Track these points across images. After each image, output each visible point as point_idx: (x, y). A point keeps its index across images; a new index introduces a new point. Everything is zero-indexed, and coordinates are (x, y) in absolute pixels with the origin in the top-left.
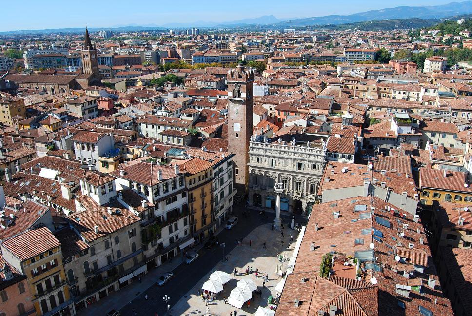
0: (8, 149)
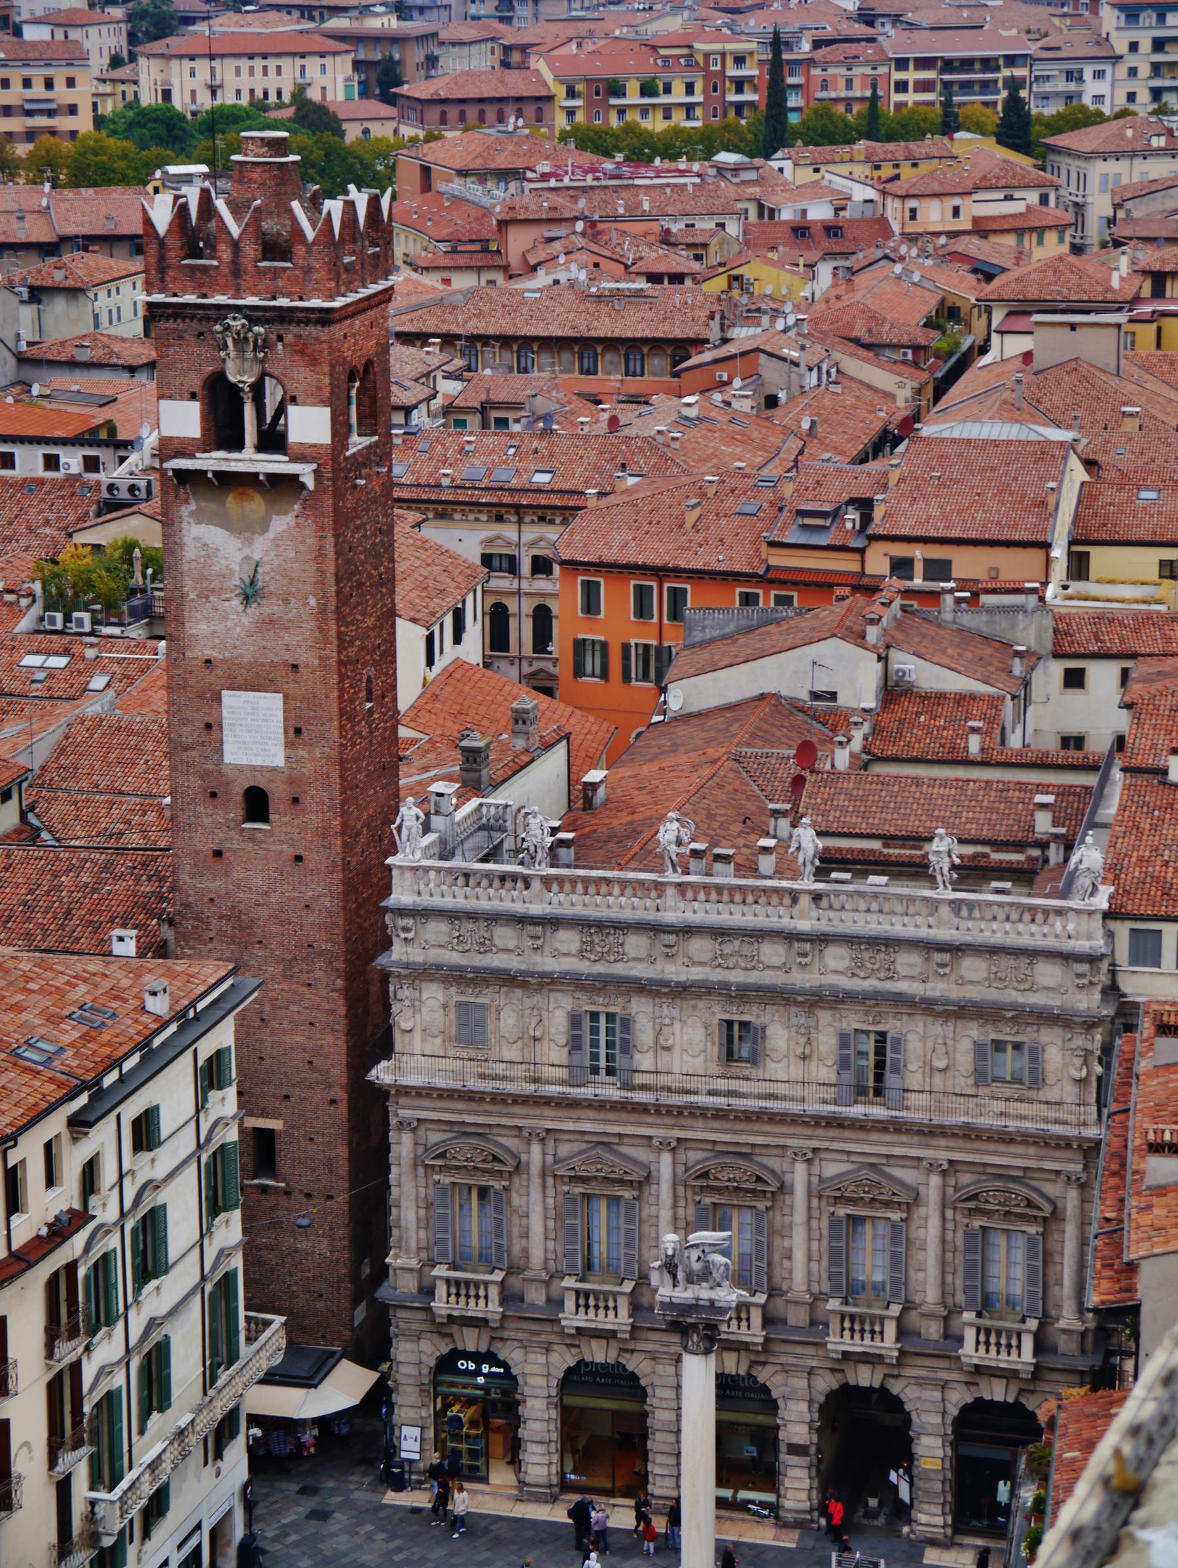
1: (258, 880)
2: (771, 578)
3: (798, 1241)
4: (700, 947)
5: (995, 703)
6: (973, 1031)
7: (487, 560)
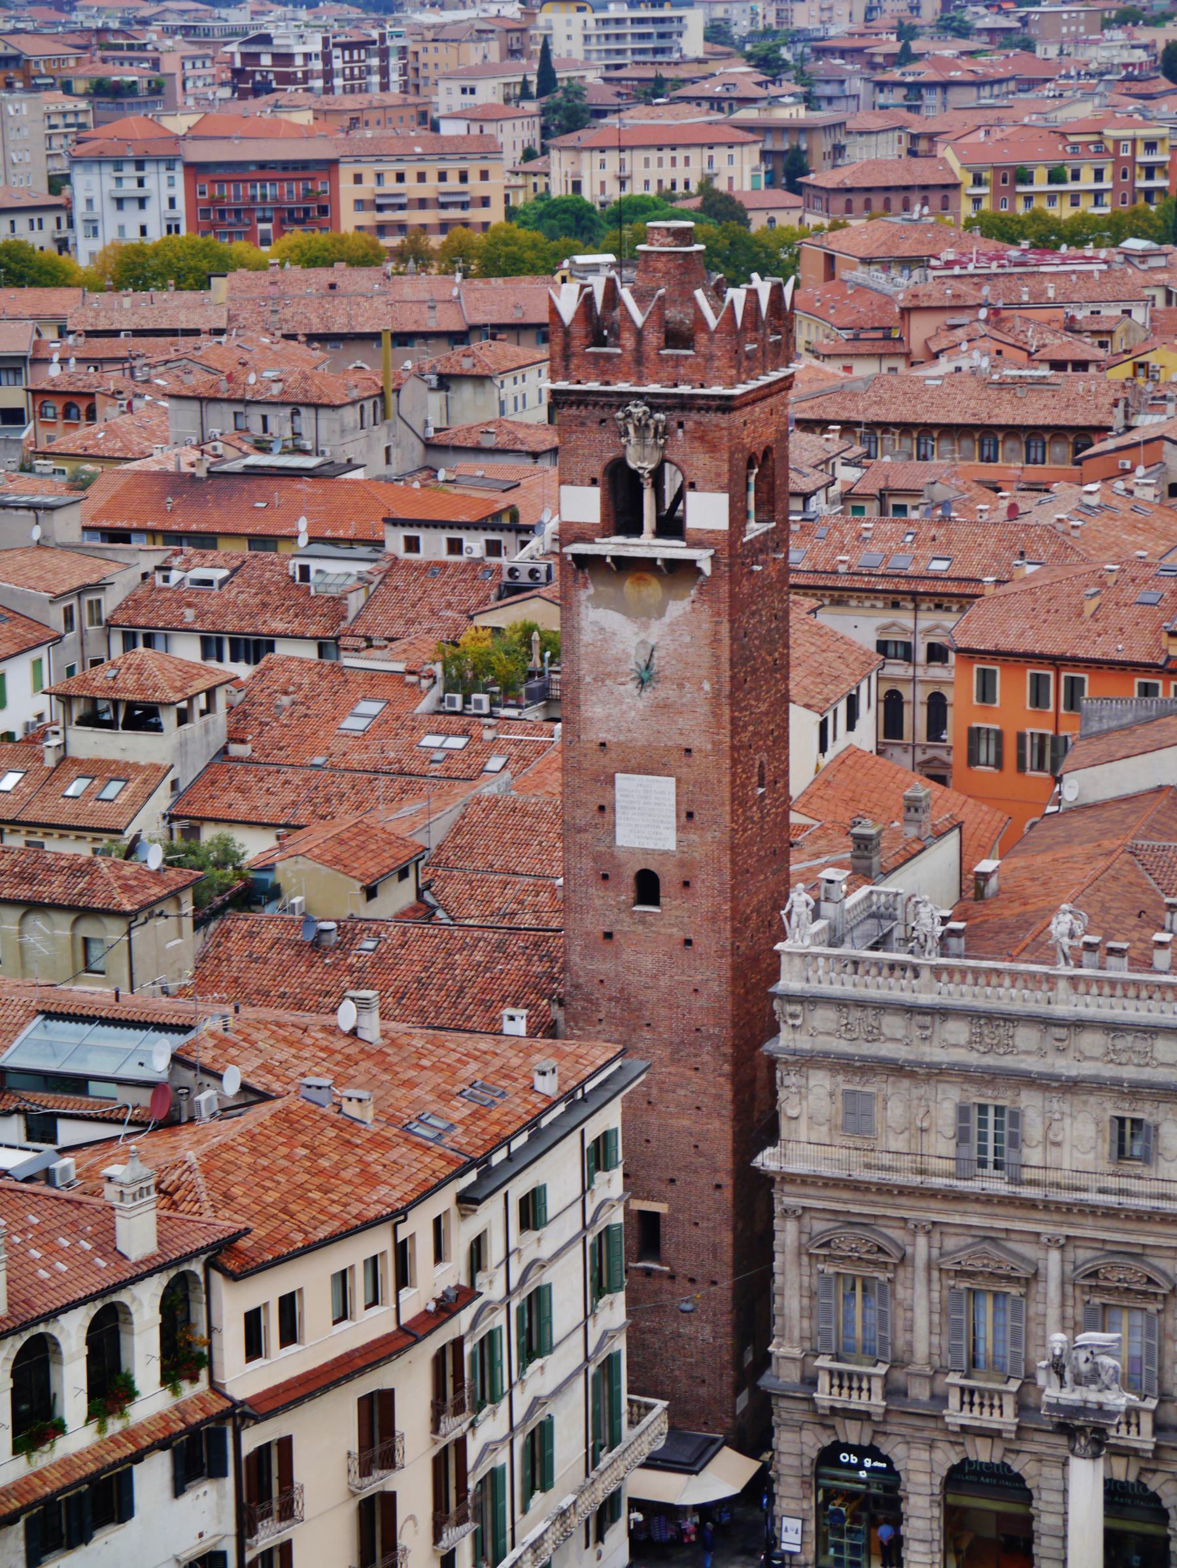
0: (500, 574)
1: (648, 963)
4: (1092, 1042)
7: (882, 647)
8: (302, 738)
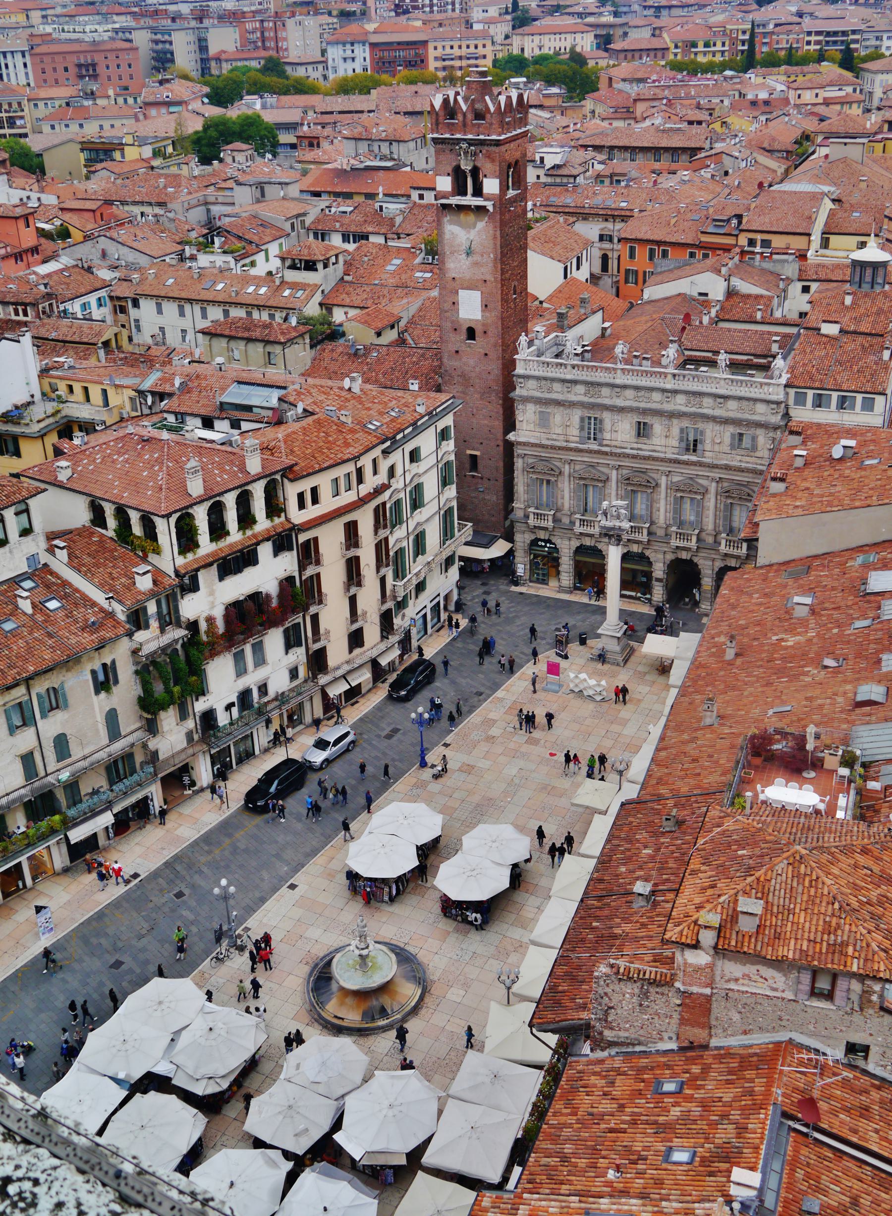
1: (472, 362)
2: (701, 246)
3: (662, 503)
4: (629, 393)
5: (770, 299)
6: (731, 429)
8: (371, 273)
